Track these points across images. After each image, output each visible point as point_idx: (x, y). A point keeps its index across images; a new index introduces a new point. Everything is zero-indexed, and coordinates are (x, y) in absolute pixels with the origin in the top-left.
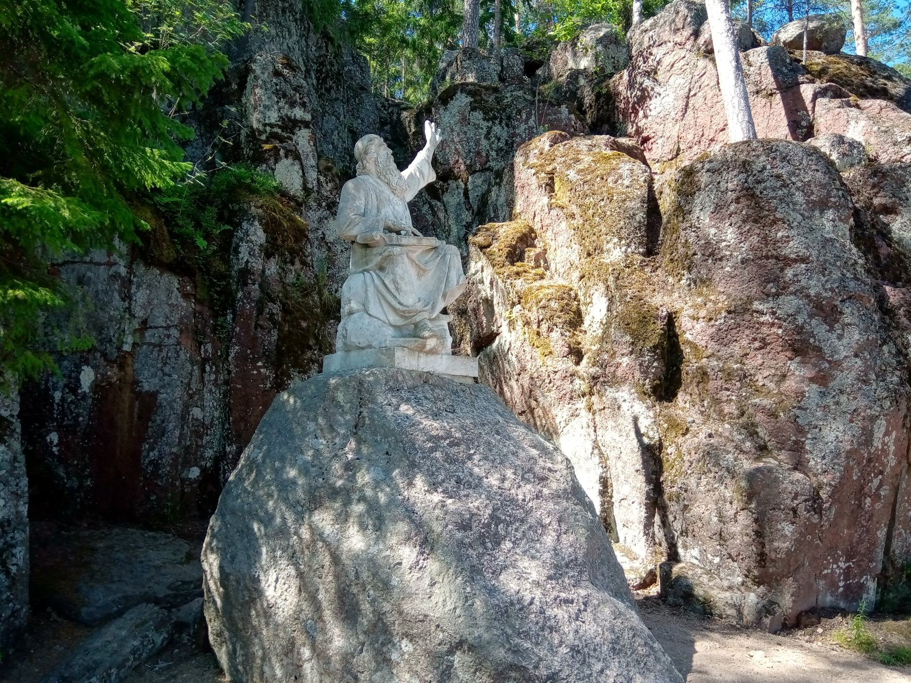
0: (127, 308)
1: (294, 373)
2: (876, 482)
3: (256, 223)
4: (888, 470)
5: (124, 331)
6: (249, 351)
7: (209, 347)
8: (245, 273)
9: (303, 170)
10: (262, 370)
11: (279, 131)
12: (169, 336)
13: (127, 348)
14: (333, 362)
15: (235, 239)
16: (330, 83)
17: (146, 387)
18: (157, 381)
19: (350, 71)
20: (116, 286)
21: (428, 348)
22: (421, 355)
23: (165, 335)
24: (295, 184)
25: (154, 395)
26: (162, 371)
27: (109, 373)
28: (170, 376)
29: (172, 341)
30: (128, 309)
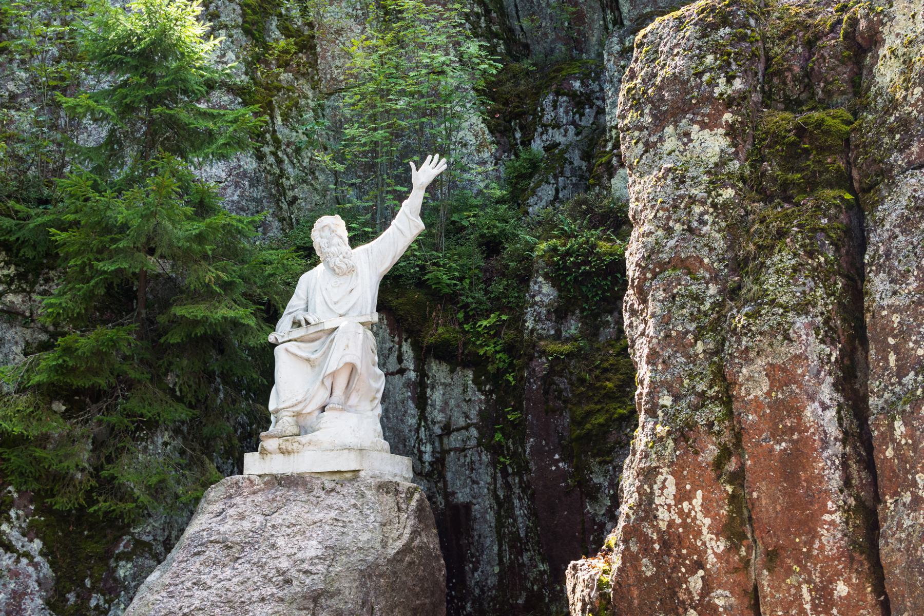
1: (594, 462)
2: (696, 583)
3: (541, 279)
4: (711, 558)
6: (544, 442)
10: (560, 464)
25: (468, 506)
29: (473, 442)
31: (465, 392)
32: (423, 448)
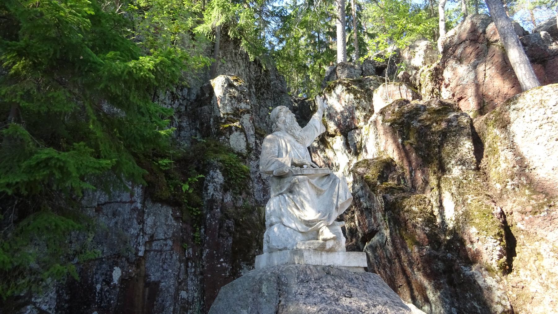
0: (141, 229)
1: (243, 265)
3: (218, 171)
5: (139, 243)
6: (215, 252)
7: (190, 250)
8: (212, 201)
9: (246, 138)
10: (223, 264)
11: (232, 117)
12: (166, 245)
13: (141, 254)
14: (262, 261)
15: (205, 182)
16: (263, 90)
17: (153, 278)
18: (159, 274)
19: (275, 83)
20: (135, 216)
21: (328, 247)
22: (323, 253)
23: (164, 244)
24: (242, 146)
25: (157, 284)
26: (162, 267)
27: (130, 271)
28: (167, 270)
29: (168, 248)
30: (142, 230)
31: (166, 220)
32: (140, 248)
